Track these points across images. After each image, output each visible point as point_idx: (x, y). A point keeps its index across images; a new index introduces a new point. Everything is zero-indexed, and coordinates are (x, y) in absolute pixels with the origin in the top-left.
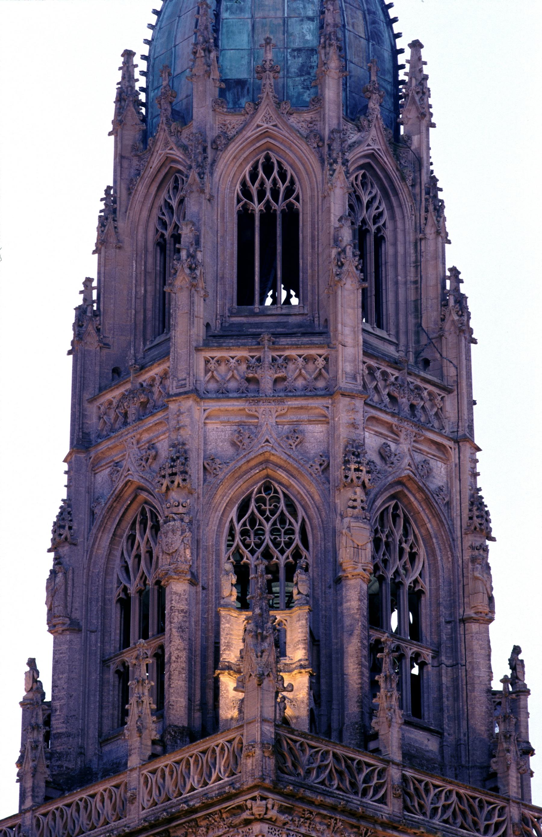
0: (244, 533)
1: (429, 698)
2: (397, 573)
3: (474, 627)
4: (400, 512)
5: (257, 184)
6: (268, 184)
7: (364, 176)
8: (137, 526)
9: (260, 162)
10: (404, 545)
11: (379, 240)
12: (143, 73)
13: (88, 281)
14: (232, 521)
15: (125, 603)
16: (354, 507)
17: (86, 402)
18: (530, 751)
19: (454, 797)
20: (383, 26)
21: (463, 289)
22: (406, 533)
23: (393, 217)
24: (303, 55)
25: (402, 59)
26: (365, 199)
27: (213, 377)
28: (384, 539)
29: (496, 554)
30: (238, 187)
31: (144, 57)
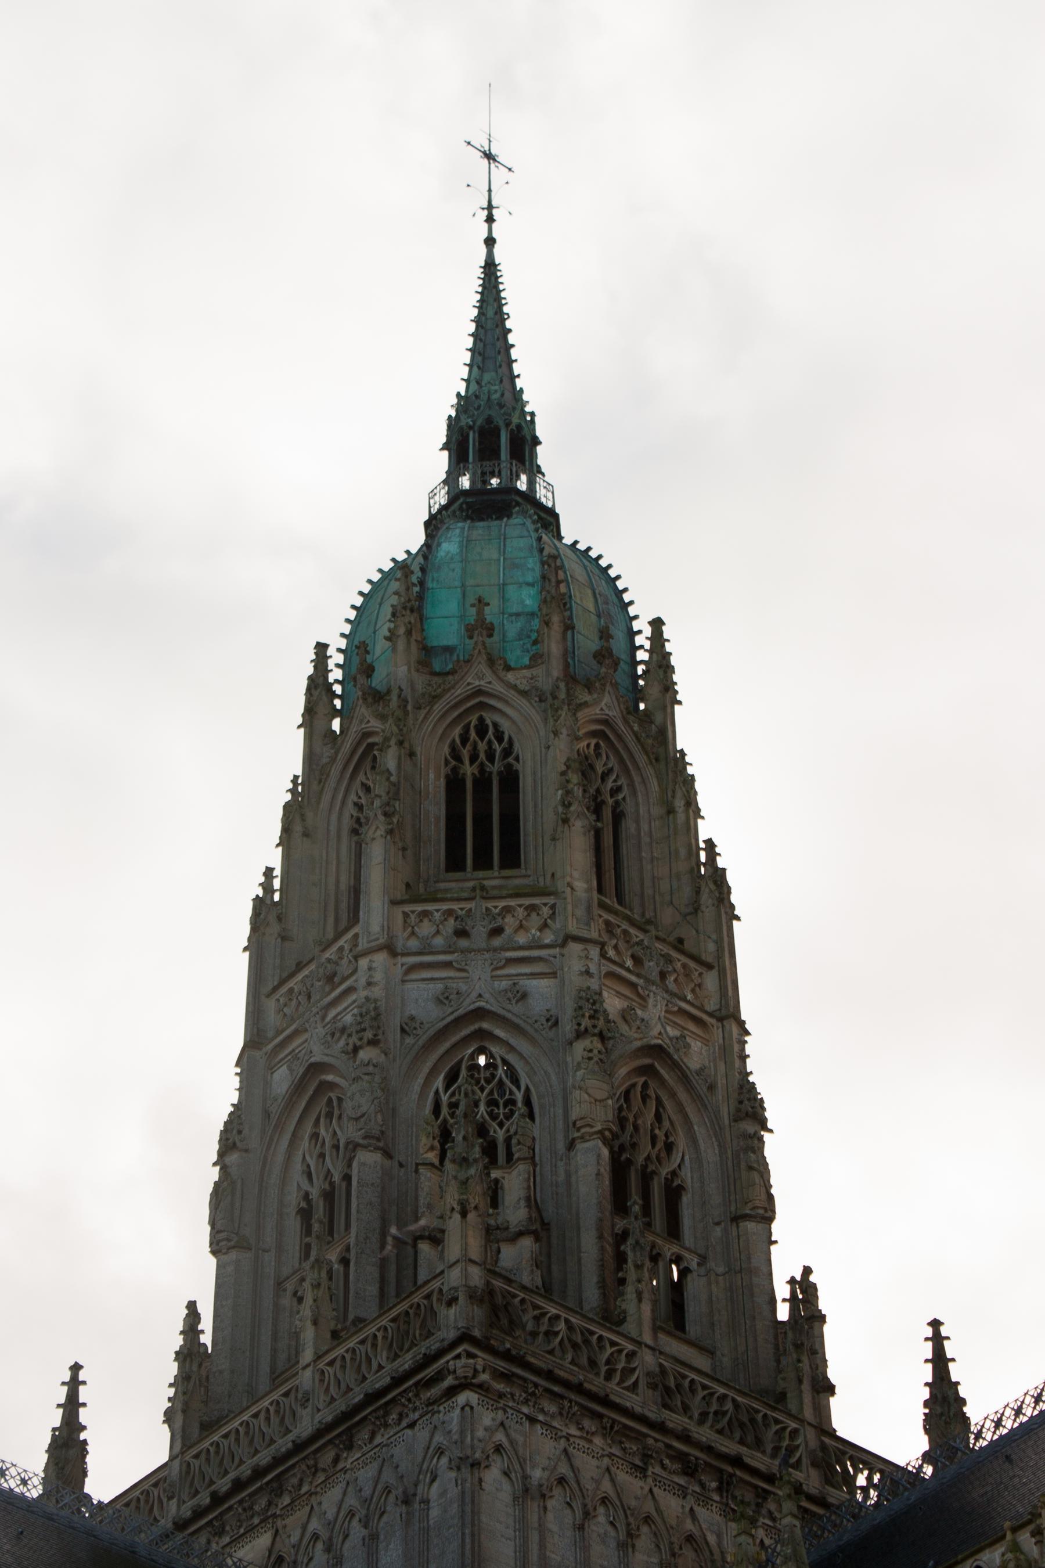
0: (454, 1106)
1: (693, 1310)
2: (648, 1158)
3: (750, 1226)
4: (651, 1092)
5: (468, 747)
6: (482, 746)
7: (597, 746)
8: (322, 1120)
9: (472, 724)
10: (657, 1131)
11: (618, 817)
12: (338, 665)
13: (269, 872)
14: (437, 1092)
15: (306, 1214)
16: (590, 1059)
17: (263, 997)
18: (831, 1389)
19: (729, 1406)
20: (614, 610)
21: (721, 863)
22: (658, 1117)
23: (634, 793)
24: (522, 619)
25: (639, 640)
26: (600, 770)
27: (413, 933)
28: (631, 1119)
29: (773, 1148)
30: (446, 750)
31: (339, 650)
